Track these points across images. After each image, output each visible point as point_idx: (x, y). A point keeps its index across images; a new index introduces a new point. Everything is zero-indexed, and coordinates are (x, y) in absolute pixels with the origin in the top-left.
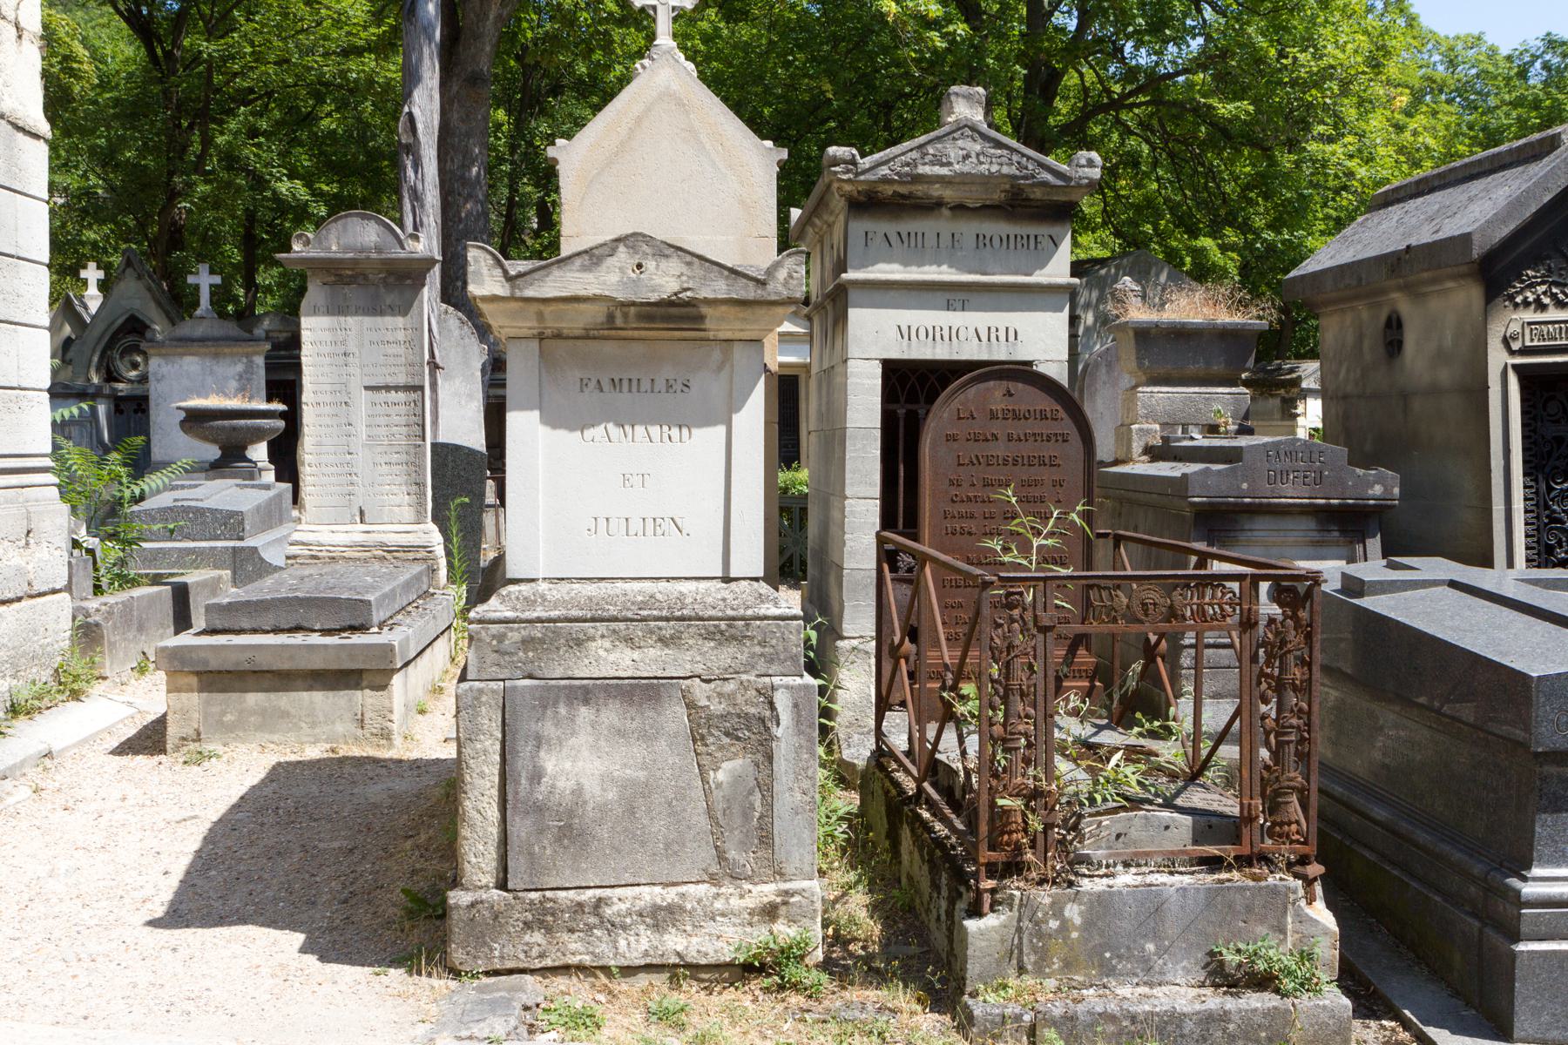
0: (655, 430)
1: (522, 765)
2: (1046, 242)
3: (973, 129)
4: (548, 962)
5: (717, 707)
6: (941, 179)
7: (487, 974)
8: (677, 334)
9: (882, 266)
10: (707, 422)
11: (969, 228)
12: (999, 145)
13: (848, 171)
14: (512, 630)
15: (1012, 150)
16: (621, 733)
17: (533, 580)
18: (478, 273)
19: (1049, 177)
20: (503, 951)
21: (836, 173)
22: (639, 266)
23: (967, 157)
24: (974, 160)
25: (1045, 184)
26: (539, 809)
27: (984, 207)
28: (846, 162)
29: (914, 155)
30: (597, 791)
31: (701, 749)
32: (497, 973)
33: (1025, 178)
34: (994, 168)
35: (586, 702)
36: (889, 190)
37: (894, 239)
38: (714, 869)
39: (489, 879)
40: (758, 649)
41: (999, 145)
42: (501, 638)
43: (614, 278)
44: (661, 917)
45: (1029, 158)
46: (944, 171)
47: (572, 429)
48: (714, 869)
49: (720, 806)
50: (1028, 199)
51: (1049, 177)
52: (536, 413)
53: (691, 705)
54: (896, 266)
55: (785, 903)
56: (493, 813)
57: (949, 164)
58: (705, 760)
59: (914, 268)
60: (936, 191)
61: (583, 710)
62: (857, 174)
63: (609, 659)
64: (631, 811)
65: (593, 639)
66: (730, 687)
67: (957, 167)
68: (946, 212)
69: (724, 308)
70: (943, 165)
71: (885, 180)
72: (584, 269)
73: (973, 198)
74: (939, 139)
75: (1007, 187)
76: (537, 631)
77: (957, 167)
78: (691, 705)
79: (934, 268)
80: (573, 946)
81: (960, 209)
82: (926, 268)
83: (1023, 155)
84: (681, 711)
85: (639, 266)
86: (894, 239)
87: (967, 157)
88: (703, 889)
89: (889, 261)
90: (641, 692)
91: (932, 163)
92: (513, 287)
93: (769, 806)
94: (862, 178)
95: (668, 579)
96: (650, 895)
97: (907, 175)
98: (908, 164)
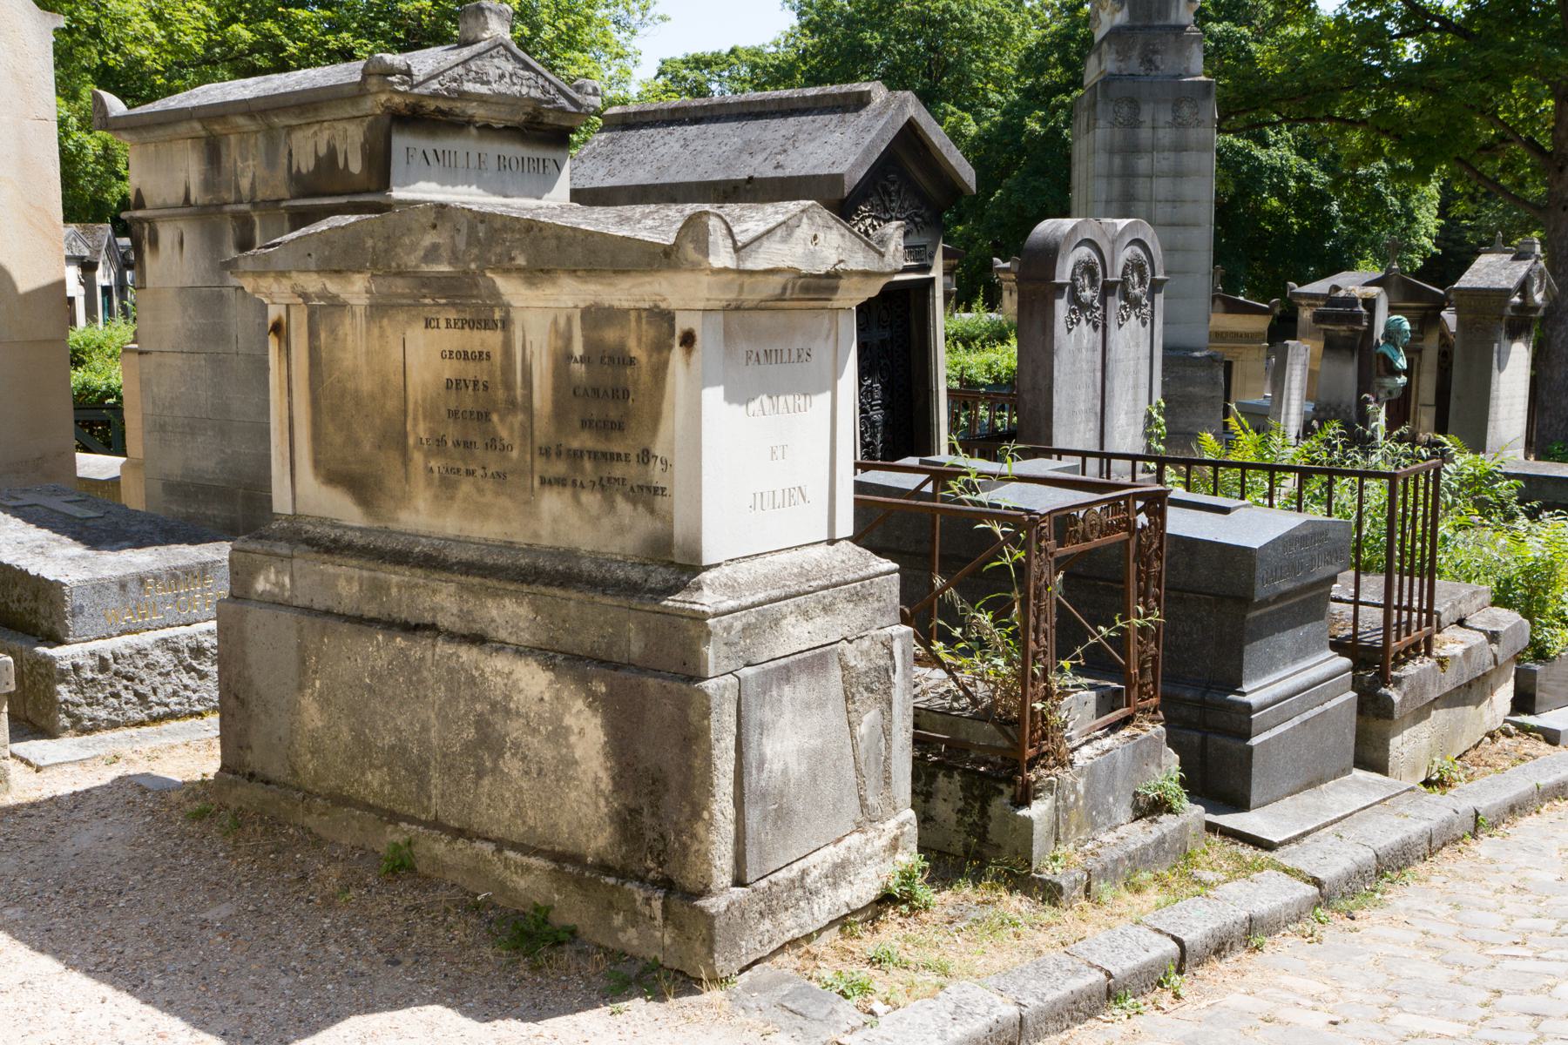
0: (790, 398)
1: (752, 756)
2: (551, 166)
3: (507, 48)
4: (775, 946)
5: (862, 665)
6: (481, 99)
7: (742, 971)
8: (812, 304)
9: (422, 185)
10: (820, 390)
11: (495, 149)
12: (527, 67)
13: (403, 83)
14: (736, 619)
15: (538, 73)
16: (808, 706)
17: (719, 565)
18: (715, 243)
19: (563, 102)
20: (750, 947)
21: (392, 83)
22: (815, 237)
23: (502, 76)
24: (507, 80)
25: (562, 110)
26: (764, 796)
27: (506, 128)
28: (401, 72)
29: (460, 70)
30: (796, 768)
31: (851, 707)
32: (749, 967)
33: (548, 102)
34: (525, 90)
35: (788, 680)
36: (432, 105)
37: (431, 157)
38: (860, 818)
39: (727, 880)
40: (876, 605)
41: (527, 67)
42: (728, 629)
43: (799, 250)
44: (838, 873)
45: (551, 83)
46: (484, 89)
47: (741, 404)
48: (860, 818)
49: (863, 757)
50: (541, 123)
51: (563, 102)
52: (721, 388)
53: (845, 667)
54: (433, 186)
55: (902, 834)
56: (730, 811)
57: (488, 83)
58: (853, 717)
59: (449, 188)
60: (473, 109)
61: (787, 689)
62: (413, 87)
63: (798, 634)
64: (814, 779)
65: (784, 617)
66: (866, 643)
67: (495, 86)
68: (473, 131)
69: (855, 279)
70: (483, 83)
71: (435, 95)
72: (784, 240)
73: (499, 117)
74: (479, 55)
75: (530, 110)
76: (751, 615)
77: (495, 86)
78: (845, 667)
79: (465, 188)
80: (788, 924)
81: (486, 129)
82: (459, 189)
83: (547, 79)
84: (838, 673)
85: (815, 237)
86: (431, 157)
87: (502, 76)
88: (856, 839)
89: (429, 180)
90: (815, 661)
91: (475, 81)
92: (739, 259)
93: (888, 748)
94: (416, 91)
95: (797, 548)
96: (831, 854)
97: (455, 91)
98: (455, 80)
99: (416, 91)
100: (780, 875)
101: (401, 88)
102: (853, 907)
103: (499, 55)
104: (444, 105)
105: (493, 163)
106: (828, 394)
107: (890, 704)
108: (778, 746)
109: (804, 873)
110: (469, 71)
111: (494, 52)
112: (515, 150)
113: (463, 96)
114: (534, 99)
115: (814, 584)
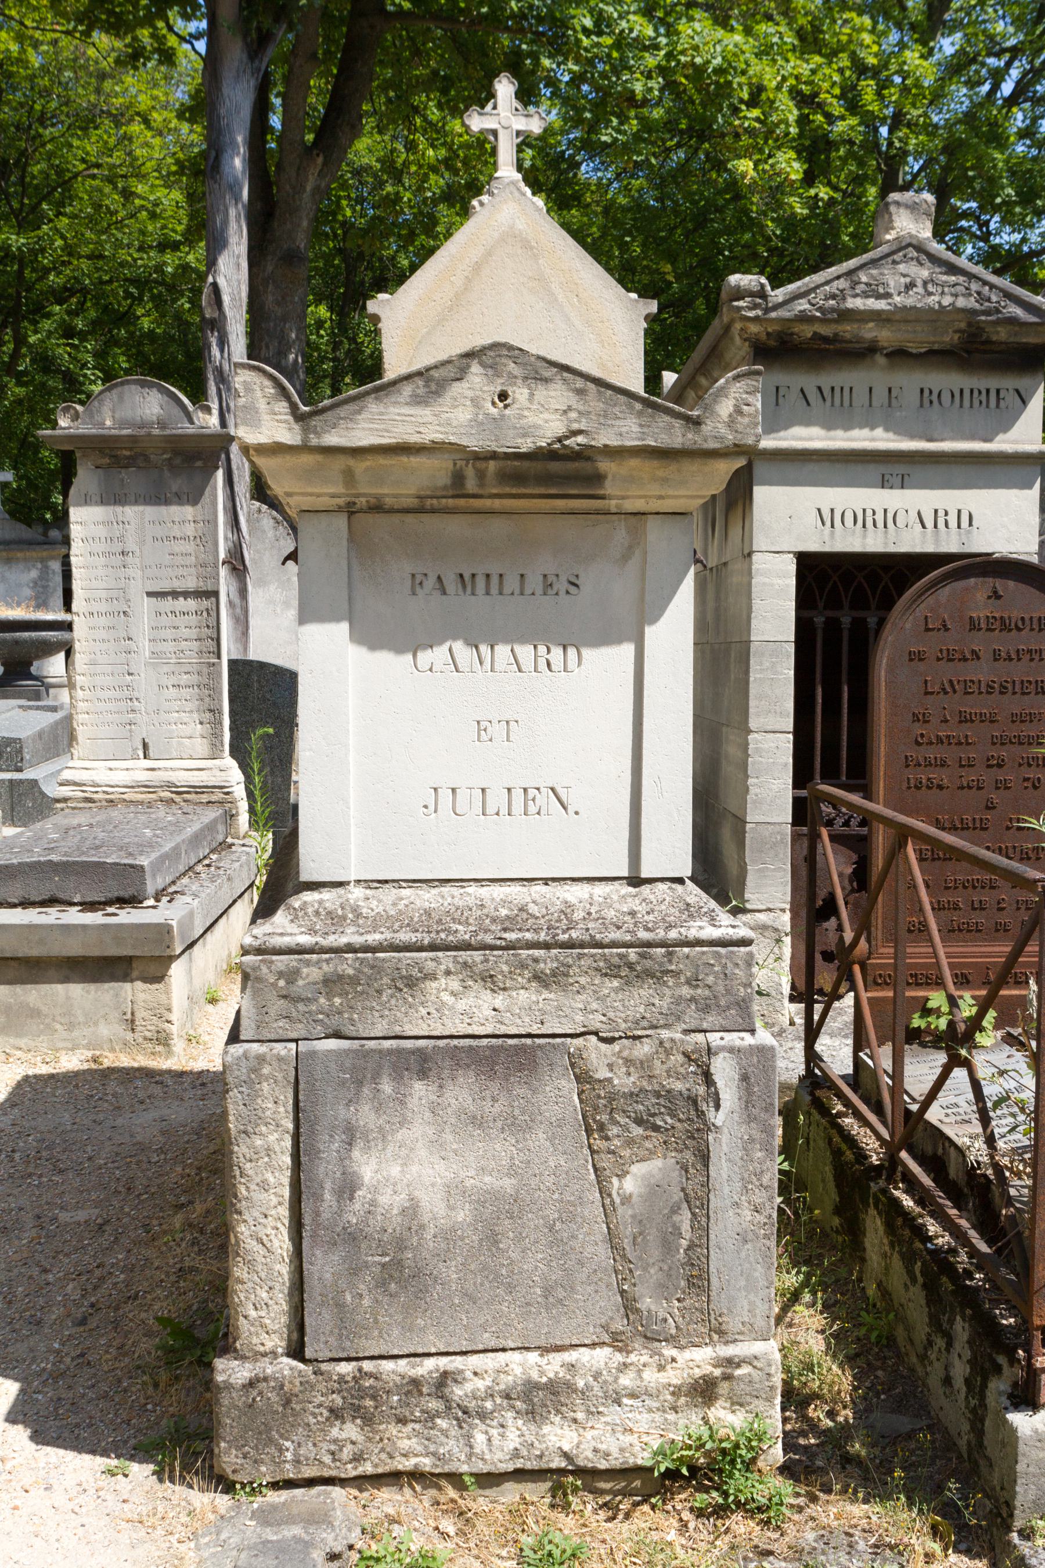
0: (525, 652)
1: (325, 1171)
2: (1011, 398)
3: (920, 248)
4: (368, 1468)
5: (624, 1081)
6: (876, 316)
7: (275, 1486)
8: (560, 503)
9: (797, 431)
10: (605, 638)
11: (910, 381)
12: (953, 269)
13: (755, 306)
14: (308, 963)
15: (971, 276)
16: (477, 1121)
17: (340, 884)
18: (251, 409)
19: (1018, 312)
20: (295, 1453)
21: (739, 309)
22: (503, 396)
23: (911, 285)
24: (920, 289)
25: (1013, 321)
26: (353, 1238)
27: (931, 353)
28: (752, 294)
29: (842, 284)
30: (441, 1210)
31: (599, 1144)
32: (290, 1484)
33: (987, 313)
34: (947, 301)
35: (423, 1074)
36: (807, 331)
37: (813, 395)
38: (619, 1325)
39: (276, 1342)
40: (686, 991)
41: (953, 269)
42: (291, 976)
43: (463, 415)
44: (539, 1400)
45: (992, 286)
46: (881, 305)
47: (399, 650)
48: (619, 1325)
49: (628, 1231)
50: (989, 342)
51: (1018, 312)
52: (344, 627)
53: (583, 1078)
54: (816, 431)
55: (727, 1377)
56: (282, 1243)
57: (887, 295)
58: (606, 1162)
59: (840, 433)
60: (869, 332)
61: (419, 1088)
62: (767, 310)
63: (459, 1007)
64: (493, 1239)
65: (433, 977)
66: (645, 1049)
67: (897, 299)
68: (881, 360)
69: (634, 462)
70: (879, 297)
71: (803, 318)
72: (417, 401)
73: (917, 340)
74: (874, 262)
75: (963, 325)
76: (347, 965)
77: (897, 299)
78: (583, 1078)
79: (865, 432)
80: (404, 1444)
81: (899, 356)
82: (856, 433)
83: (985, 283)
84: (569, 1086)
85: (503, 396)
86: (813, 395)
87: (911, 285)
88: (601, 1357)
89: (808, 423)
90: (506, 1059)
91: (866, 295)
92: (306, 431)
93: (702, 1229)
94: (773, 315)
95: (546, 881)
96: (523, 1365)
97: (833, 310)
98: (833, 297)
99: (773, 315)
100: (388, 1365)
101: (751, 314)
102: (581, 1462)
103: (906, 259)
104: (825, 330)
105: (912, 398)
106: (628, 649)
107: (704, 1157)
108: (395, 1171)
109: (445, 1378)
110: (855, 284)
111: (897, 257)
112: (947, 380)
113: (846, 315)
114: (963, 310)
115: (512, 936)
